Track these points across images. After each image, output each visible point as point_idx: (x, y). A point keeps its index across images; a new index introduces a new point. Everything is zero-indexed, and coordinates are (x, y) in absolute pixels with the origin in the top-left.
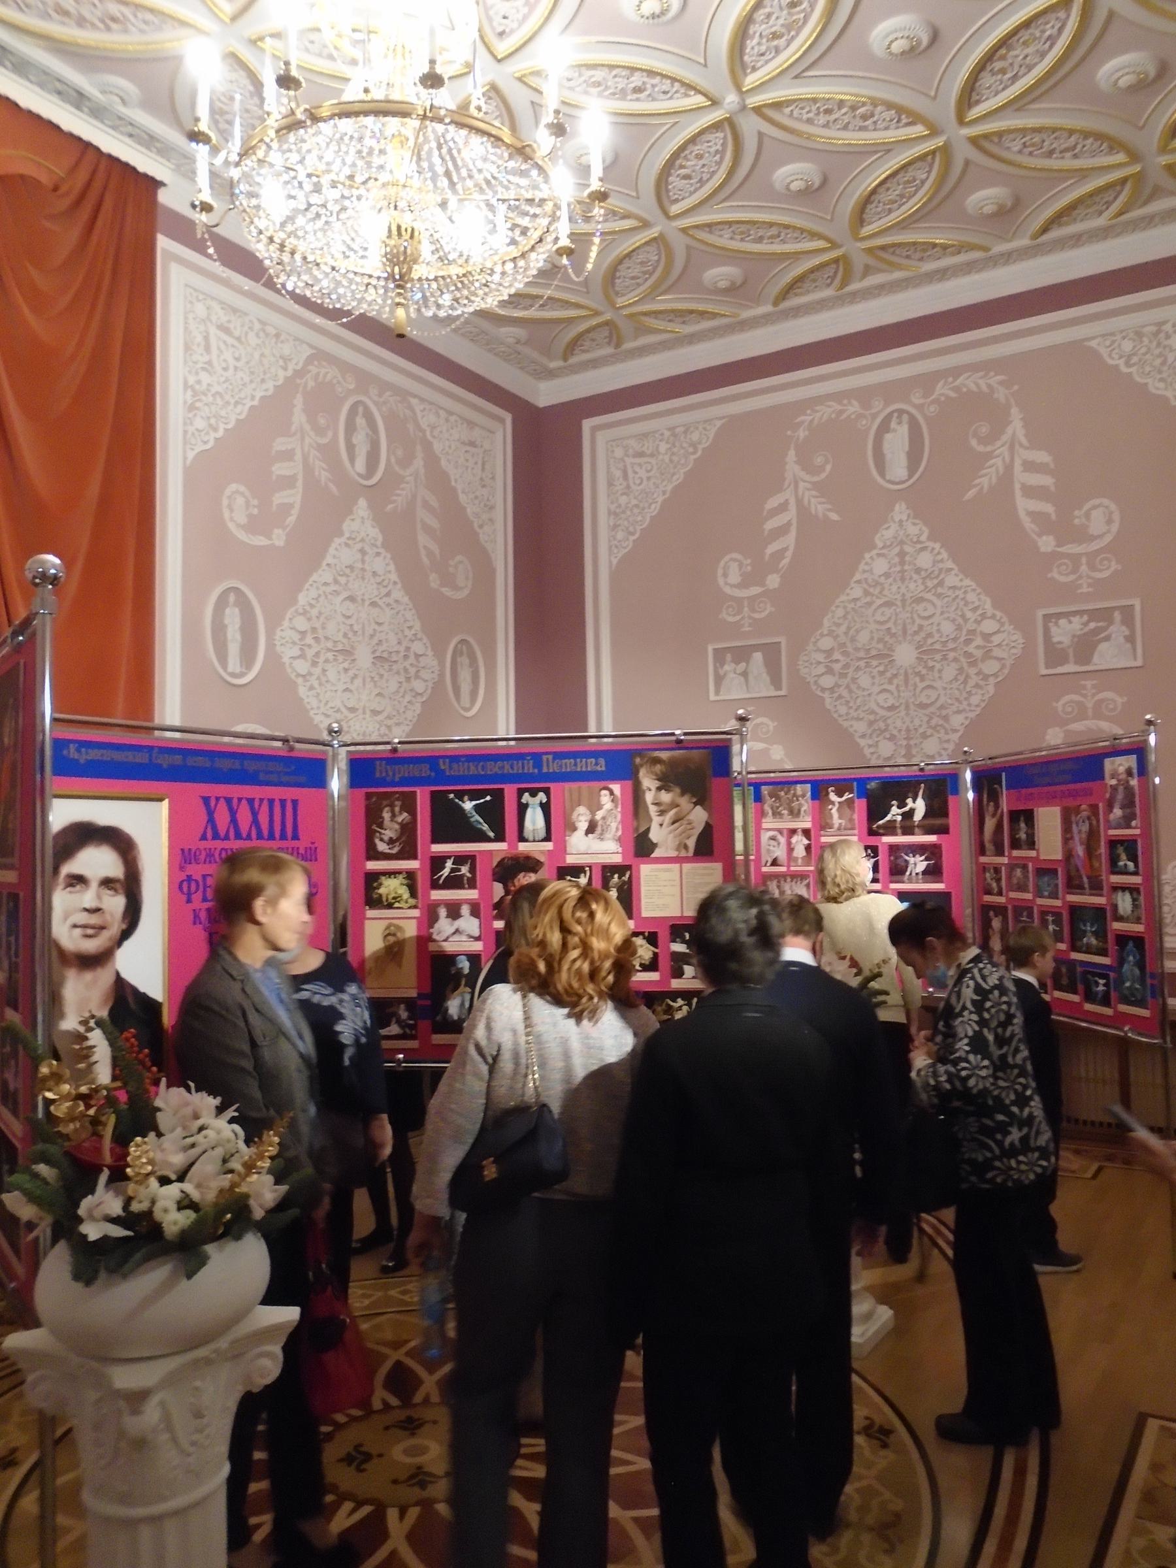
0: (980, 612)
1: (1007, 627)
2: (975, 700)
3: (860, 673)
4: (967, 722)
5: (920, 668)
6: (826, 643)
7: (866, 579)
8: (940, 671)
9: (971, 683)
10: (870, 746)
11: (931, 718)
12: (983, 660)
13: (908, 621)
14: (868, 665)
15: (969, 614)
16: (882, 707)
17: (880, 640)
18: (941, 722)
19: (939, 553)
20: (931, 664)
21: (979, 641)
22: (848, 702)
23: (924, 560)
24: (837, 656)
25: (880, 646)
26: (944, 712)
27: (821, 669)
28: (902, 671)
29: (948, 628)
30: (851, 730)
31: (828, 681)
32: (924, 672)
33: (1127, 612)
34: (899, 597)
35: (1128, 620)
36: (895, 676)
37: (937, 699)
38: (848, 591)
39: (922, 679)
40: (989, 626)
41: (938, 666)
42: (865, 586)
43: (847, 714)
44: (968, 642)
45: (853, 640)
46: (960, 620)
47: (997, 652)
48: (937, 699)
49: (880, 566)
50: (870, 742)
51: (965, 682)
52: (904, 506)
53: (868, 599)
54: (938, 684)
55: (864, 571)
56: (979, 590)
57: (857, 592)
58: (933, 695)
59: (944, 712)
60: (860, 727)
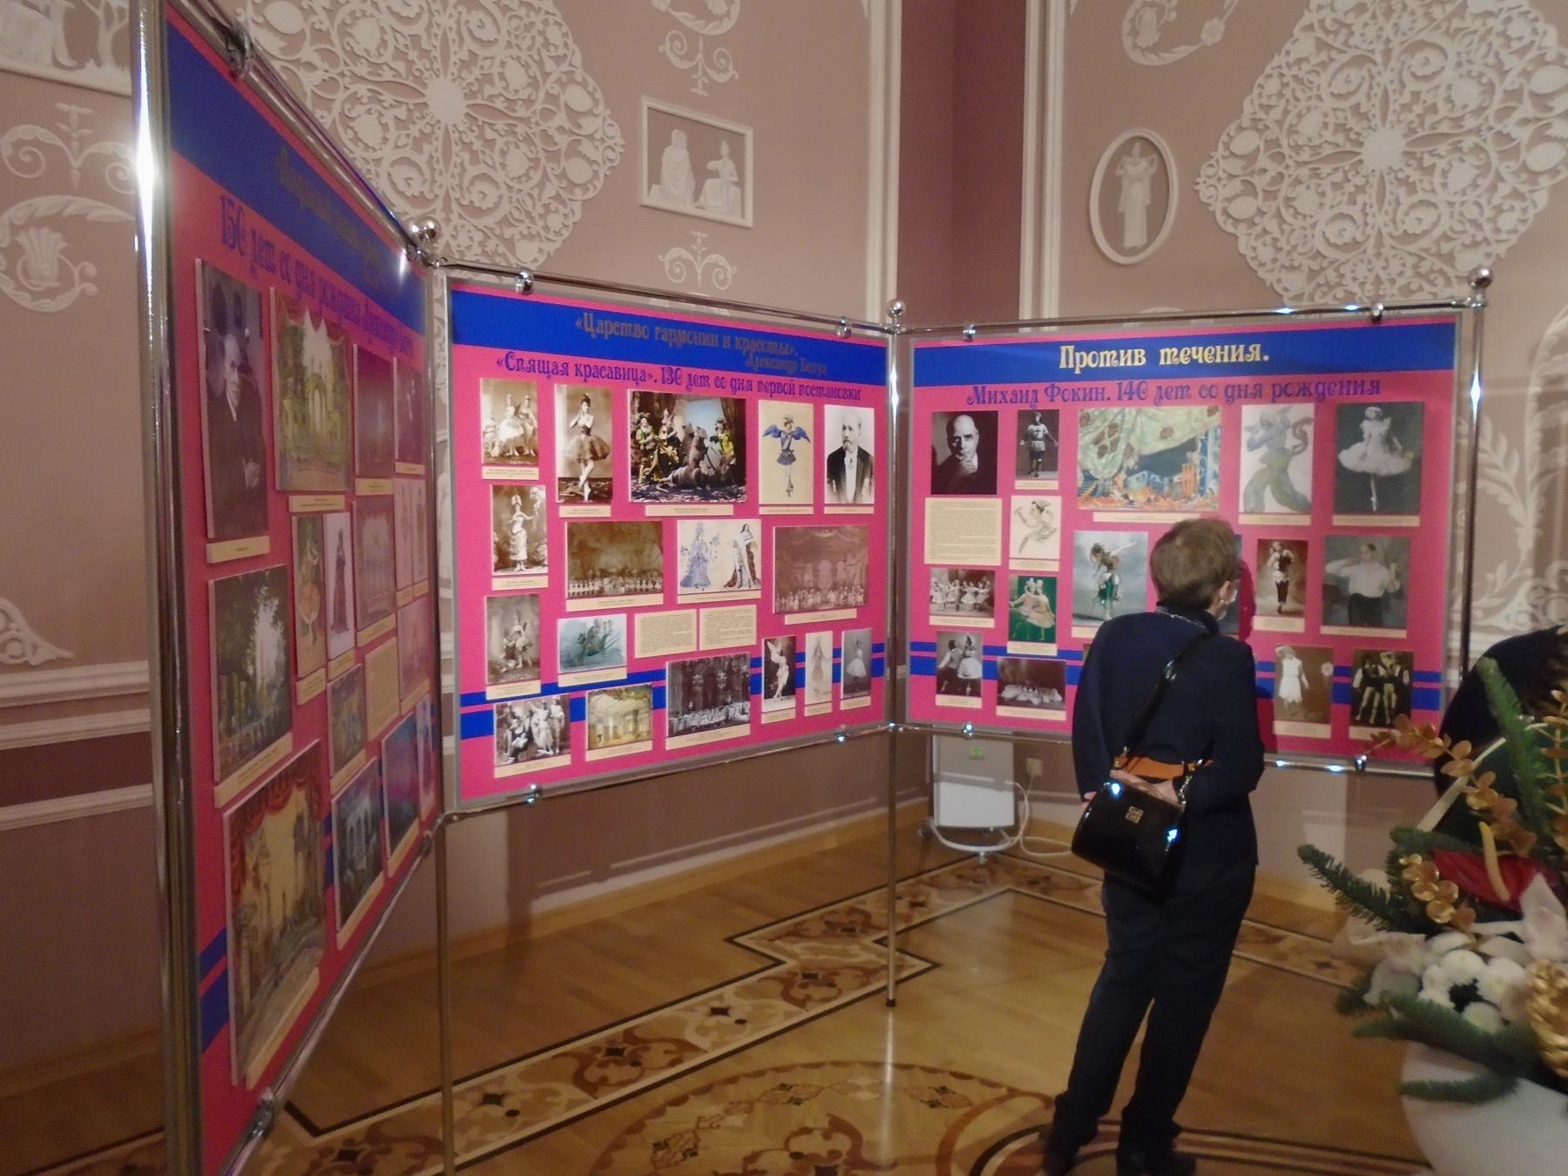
0: (565, 67)
1: (601, 109)
2: (555, 221)
3: (359, 110)
8: (503, 153)
9: (550, 190)
11: (487, 237)
12: (568, 156)
13: (452, 36)
14: (375, 97)
15: (550, 66)
16: (401, 193)
17: (400, 54)
18: (502, 249)
20: (489, 134)
21: (561, 119)
26: (508, 232)
28: (440, 133)
32: (477, 145)
33: (737, 139)
35: (738, 157)
36: (425, 137)
37: (497, 204)
39: (475, 160)
40: (577, 98)
41: (500, 143)
44: (547, 114)
46: (534, 69)
48: (497, 204)
51: (541, 185)
54: (499, 176)
56: (565, 29)
58: (493, 194)
59: (508, 232)
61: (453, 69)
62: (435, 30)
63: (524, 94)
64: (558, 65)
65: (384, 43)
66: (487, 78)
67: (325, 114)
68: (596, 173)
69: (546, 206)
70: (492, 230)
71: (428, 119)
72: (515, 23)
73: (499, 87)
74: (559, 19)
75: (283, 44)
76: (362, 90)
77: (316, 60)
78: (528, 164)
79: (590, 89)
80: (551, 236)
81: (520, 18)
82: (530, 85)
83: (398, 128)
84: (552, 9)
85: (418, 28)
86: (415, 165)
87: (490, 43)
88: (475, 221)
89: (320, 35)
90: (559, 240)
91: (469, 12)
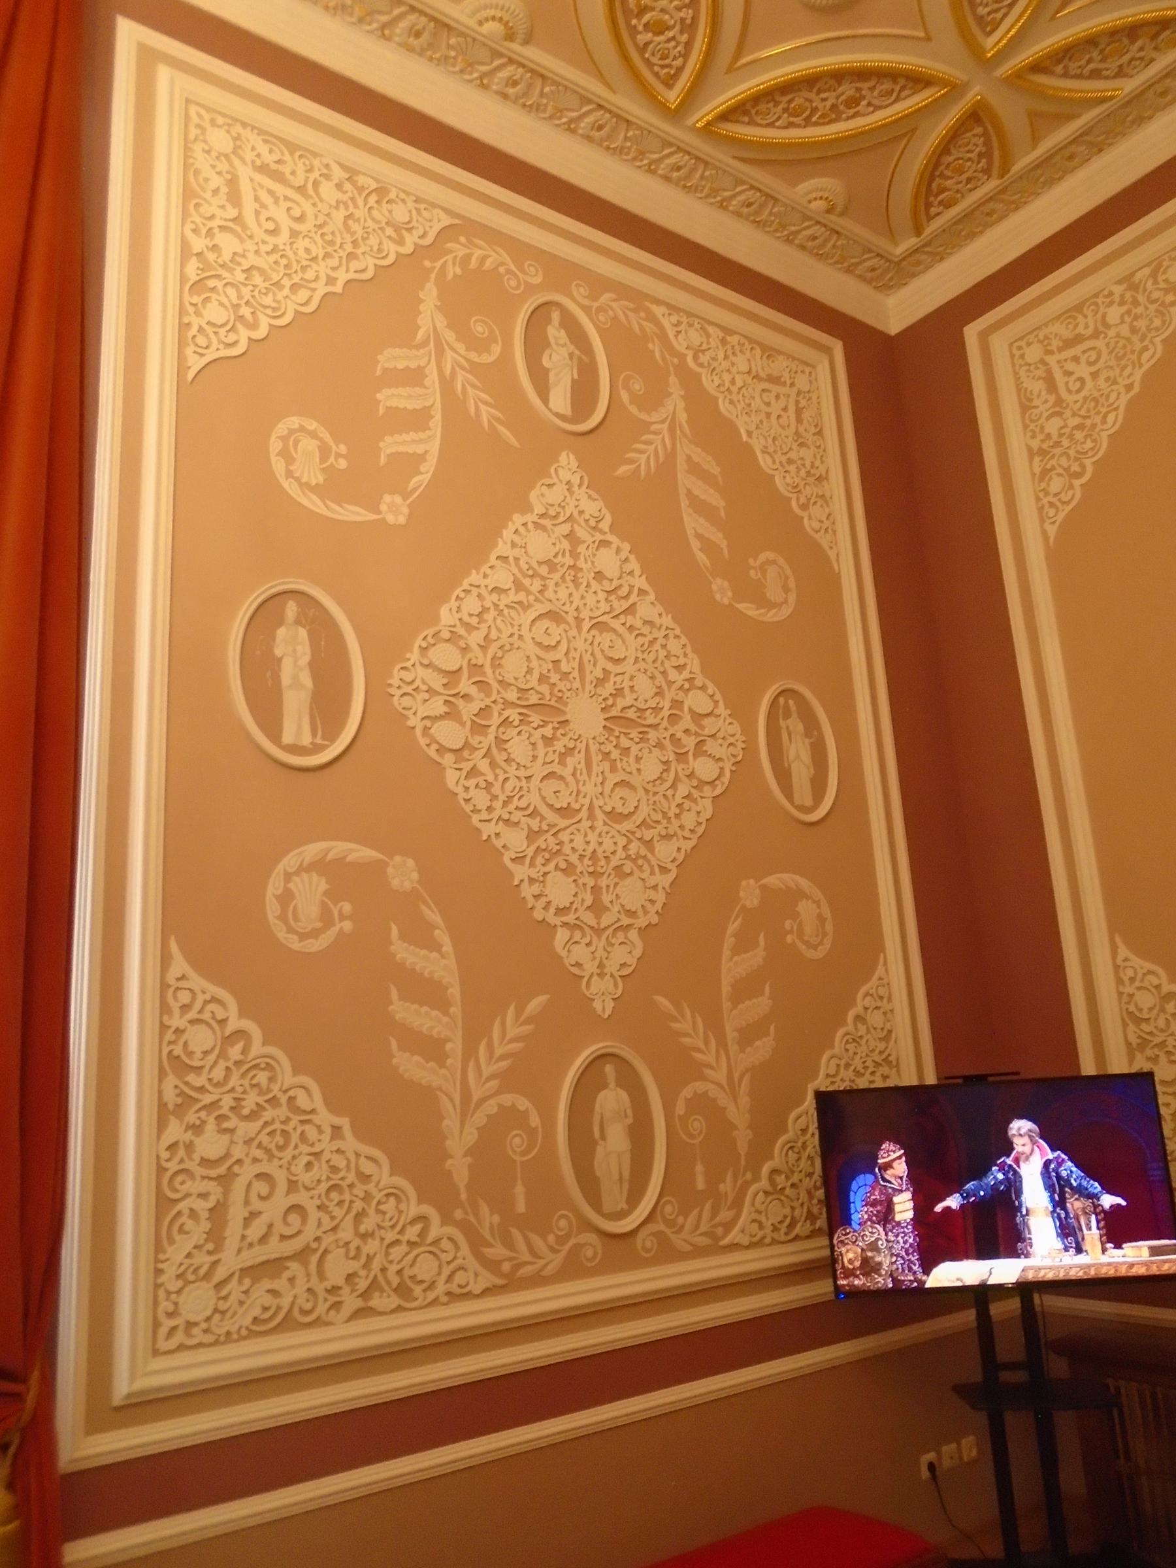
0: (686, 674)
1: (721, 710)
2: (689, 820)
4: (681, 858)
5: (608, 747)
6: (447, 657)
7: (517, 559)
9: (683, 790)
10: (532, 881)
11: (630, 841)
12: (695, 756)
16: (551, 806)
18: (643, 852)
19: (626, 560)
20: (624, 742)
22: (489, 785)
23: (608, 561)
24: (465, 686)
25: (545, 689)
27: (437, 706)
29: (645, 688)
30: (498, 844)
31: (450, 734)
32: (615, 754)
34: (571, 609)
38: (485, 568)
41: (635, 750)
42: (515, 571)
43: (490, 809)
44: (673, 718)
45: (496, 663)
46: (660, 678)
47: (711, 747)
49: (540, 545)
50: (533, 873)
51: (673, 786)
52: (574, 464)
53: (522, 596)
54: (636, 780)
55: (514, 545)
56: (684, 640)
57: (502, 577)
59: (648, 834)
60: (515, 840)
61: (588, 687)
62: (572, 654)
63: (652, 703)
64: (680, 673)
65: (529, 671)
66: (619, 692)
67: (482, 738)
68: (722, 769)
69: (679, 805)
70: (633, 833)
71: (571, 735)
72: (640, 640)
73: (629, 699)
74: (678, 631)
75: (445, 681)
76: (513, 714)
77: (473, 691)
78: (661, 767)
79: (710, 691)
80: (687, 834)
81: (644, 635)
82: (657, 694)
83: (546, 746)
84: (672, 625)
85: (559, 655)
86: (562, 778)
87: (618, 661)
88: (617, 827)
89: (475, 668)
90: (695, 837)
91: (601, 634)
